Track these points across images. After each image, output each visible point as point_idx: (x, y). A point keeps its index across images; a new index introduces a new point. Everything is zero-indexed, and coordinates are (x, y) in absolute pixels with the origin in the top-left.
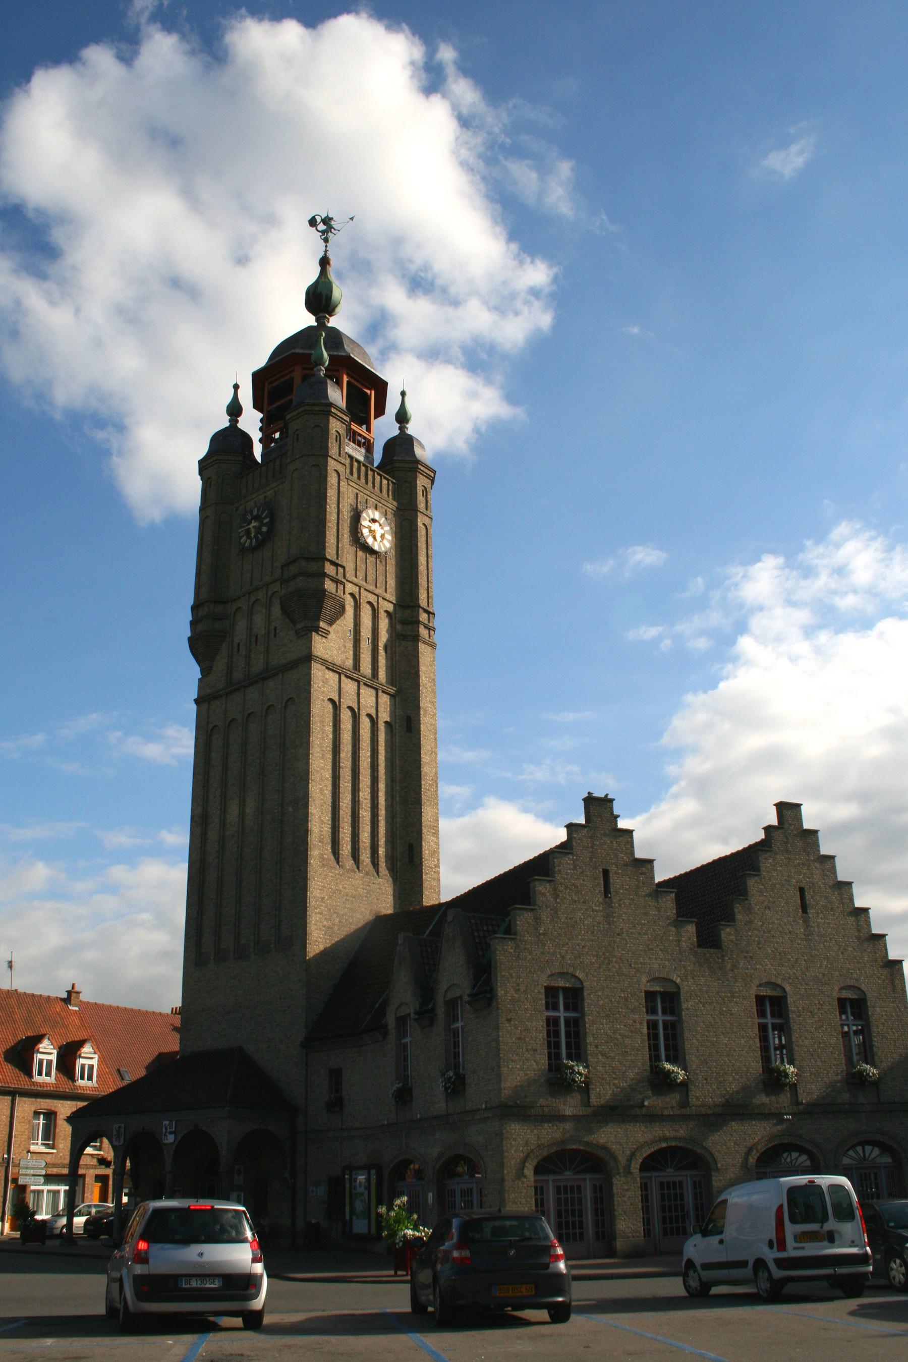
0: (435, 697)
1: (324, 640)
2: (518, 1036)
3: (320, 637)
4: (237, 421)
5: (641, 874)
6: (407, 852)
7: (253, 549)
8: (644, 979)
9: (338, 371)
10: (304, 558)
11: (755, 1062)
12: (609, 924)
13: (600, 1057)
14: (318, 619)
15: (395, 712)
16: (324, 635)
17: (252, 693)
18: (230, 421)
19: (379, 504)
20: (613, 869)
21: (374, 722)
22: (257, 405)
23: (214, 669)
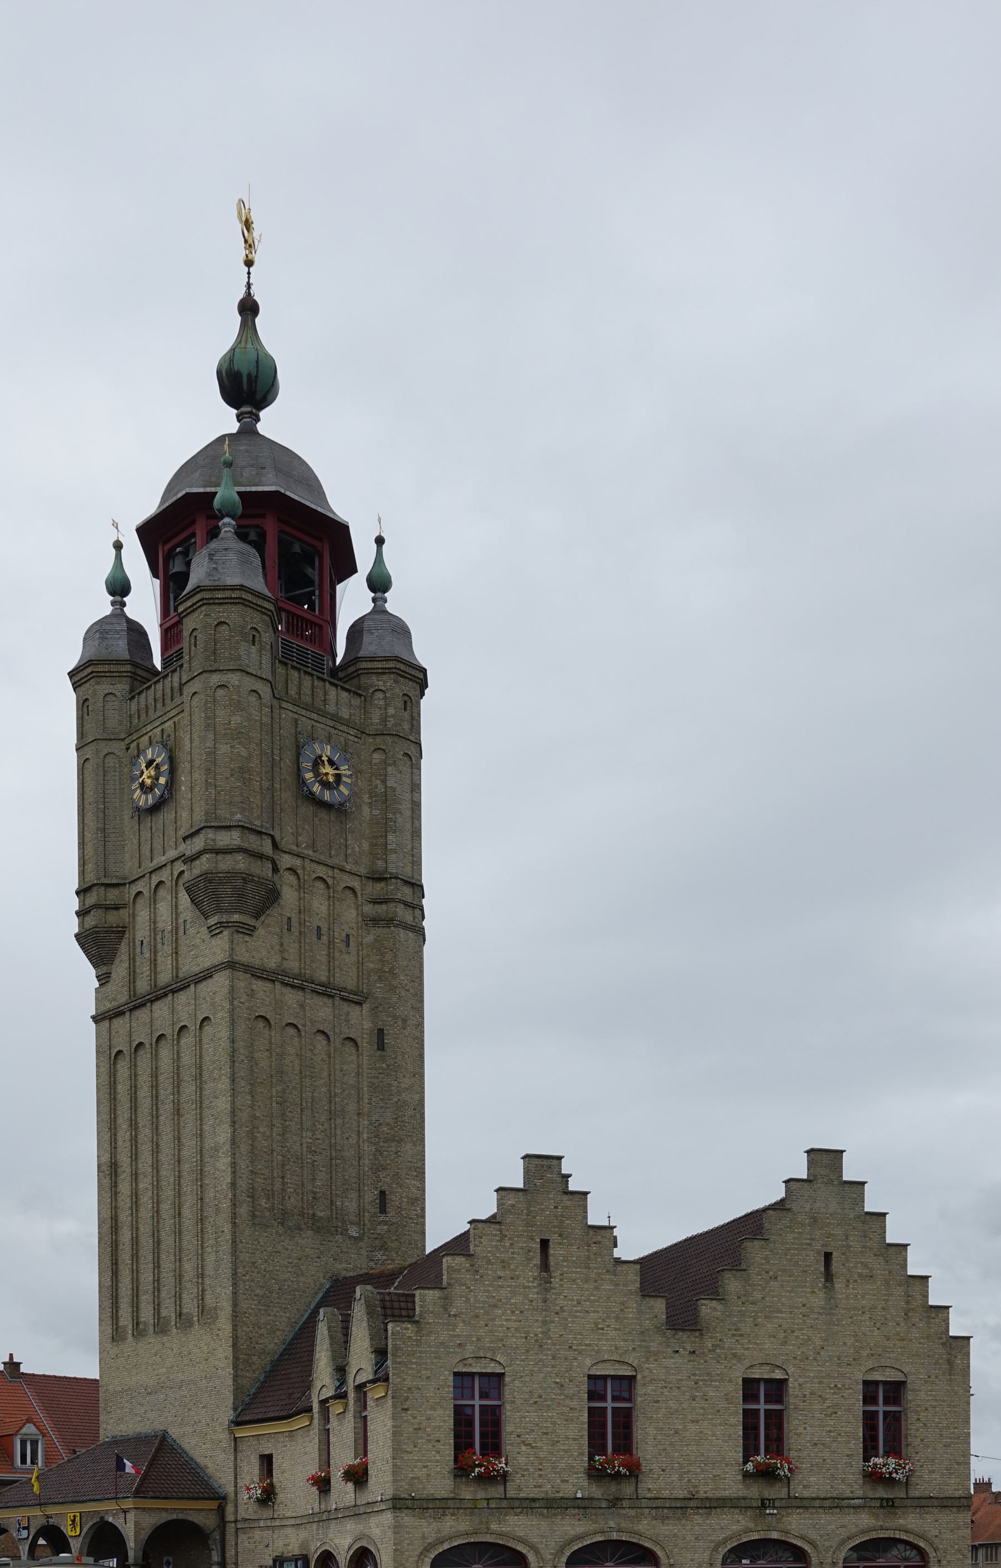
1: (247, 938)
3: (241, 935)
7: (154, 809)
8: (588, 1362)
11: (733, 1451)
13: (523, 1448)
17: (161, 1009)
19: (333, 731)
23: (114, 975)
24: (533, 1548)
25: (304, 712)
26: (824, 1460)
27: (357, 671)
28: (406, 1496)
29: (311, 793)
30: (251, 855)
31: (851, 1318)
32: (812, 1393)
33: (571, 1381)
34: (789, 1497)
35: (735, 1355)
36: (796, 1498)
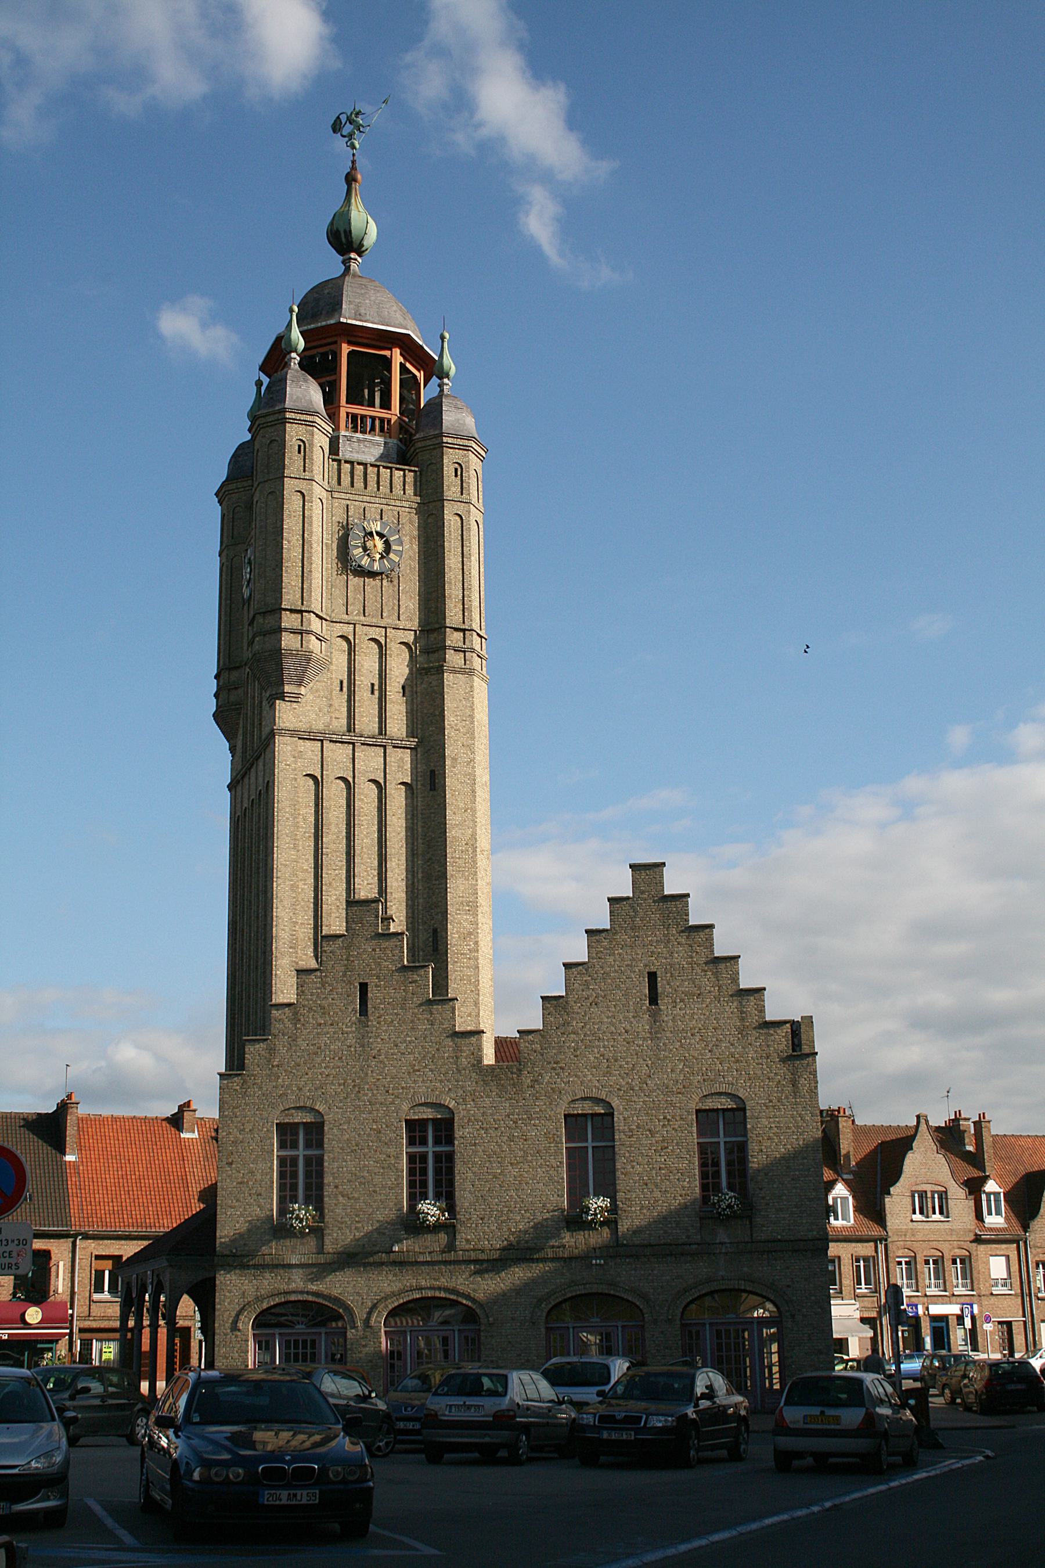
0: (473, 738)
1: (295, 705)
2: (239, 1180)
3: (289, 703)
5: (410, 983)
6: (431, 939)
8: (405, 1107)
9: (336, 342)
10: (259, 613)
11: (556, 1196)
12: (363, 1046)
13: (341, 1198)
14: (283, 685)
15: (417, 768)
16: (293, 699)
19: (385, 507)
20: (372, 982)
21: (381, 788)
27: (415, 450)
28: (228, 1253)
30: (291, 632)
34: (618, 1245)
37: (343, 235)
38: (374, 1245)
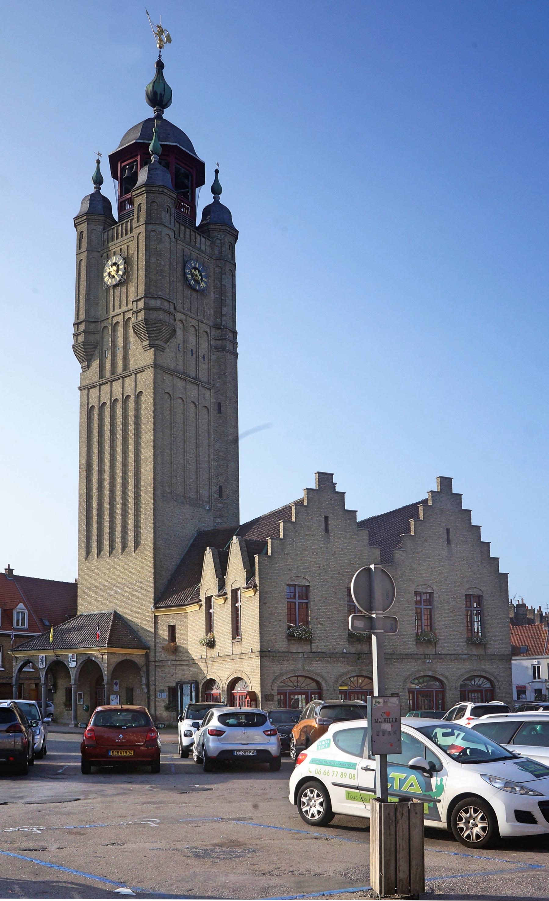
4: (100, 189)
18: (95, 188)
19: (198, 256)
22: (114, 176)
24: (324, 679)
25: (187, 246)
26: (450, 635)
28: (265, 650)
29: (190, 284)
31: (459, 562)
32: (444, 600)
33: (339, 590)
34: (436, 654)
35: (411, 580)
36: (439, 654)
37: (159, 96)
38: (335, 649)
